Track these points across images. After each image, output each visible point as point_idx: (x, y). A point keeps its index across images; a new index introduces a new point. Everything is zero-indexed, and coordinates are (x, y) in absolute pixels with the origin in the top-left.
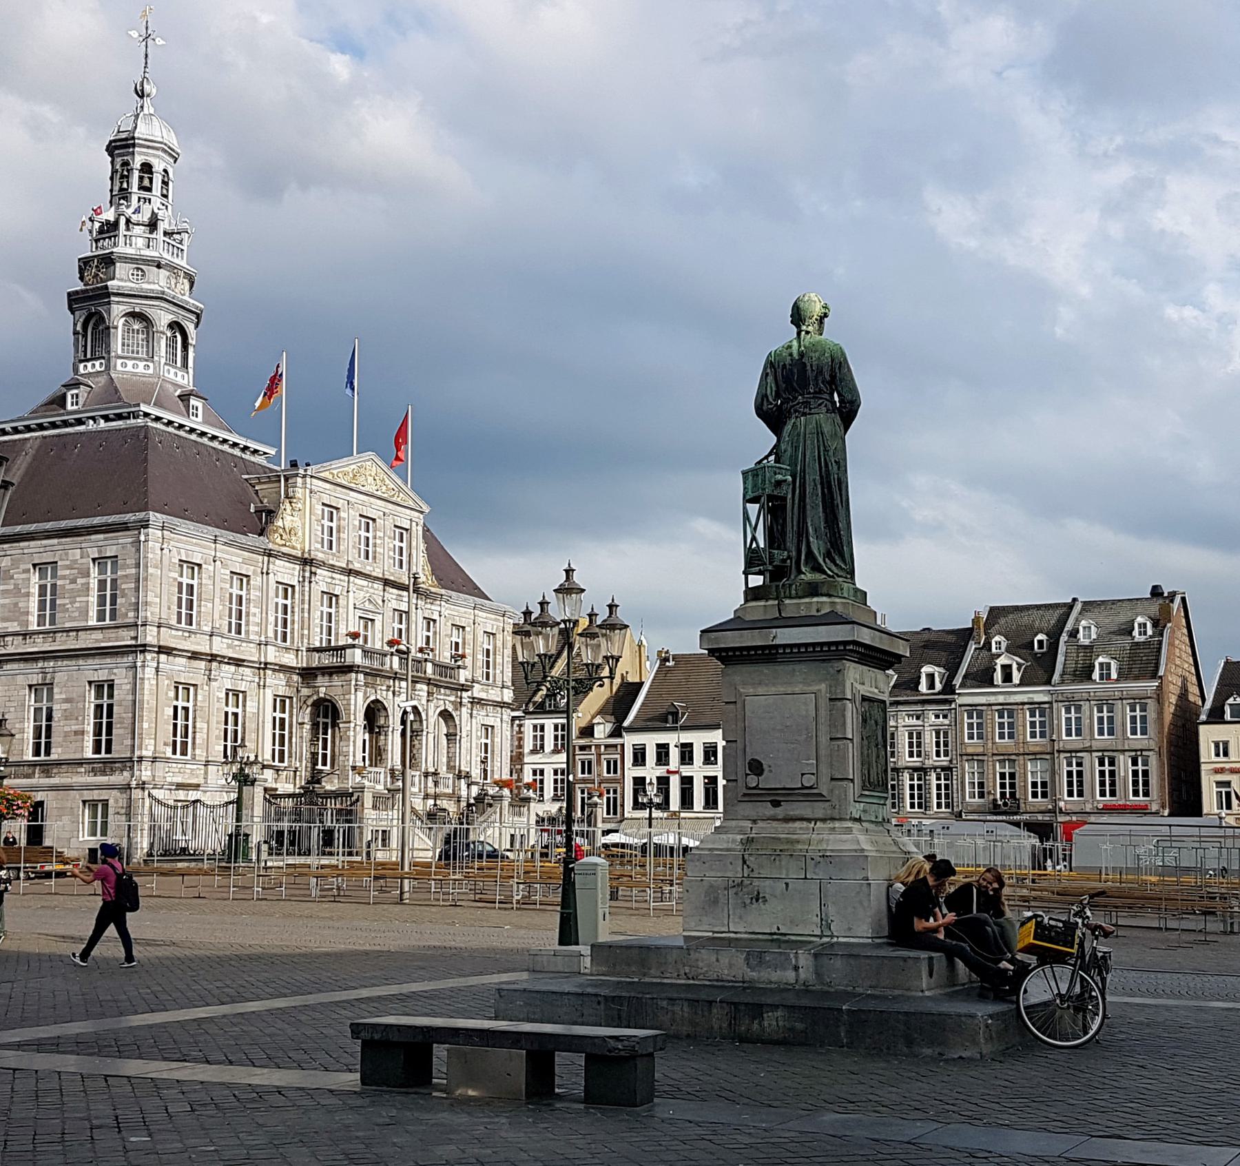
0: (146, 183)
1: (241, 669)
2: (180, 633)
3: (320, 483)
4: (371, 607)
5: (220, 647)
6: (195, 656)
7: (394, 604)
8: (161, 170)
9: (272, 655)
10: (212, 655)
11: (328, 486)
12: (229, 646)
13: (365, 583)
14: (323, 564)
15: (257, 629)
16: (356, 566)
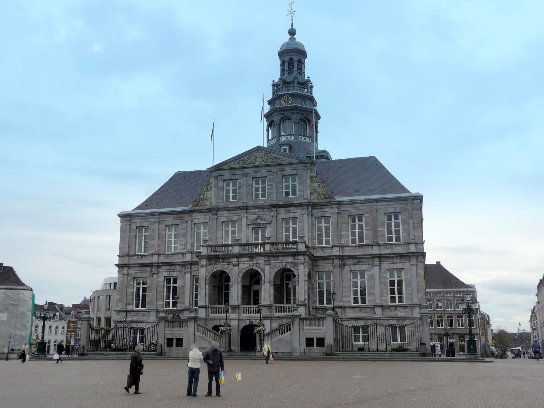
0: (291, 67)
1: (173, 267)
2: (136, 257)
3: (221, 172)
4: (263, 222)
5: (155, 259)
6: (142, 265)
7: (283, 215)
8: (297, 59)
9: (188, 258)
10: (151, 263)
11: (227, 171)
12: (165, 258)
13: (257, 210)
14: (218, 210)
15: (183, 247)
16: (250, 203)
